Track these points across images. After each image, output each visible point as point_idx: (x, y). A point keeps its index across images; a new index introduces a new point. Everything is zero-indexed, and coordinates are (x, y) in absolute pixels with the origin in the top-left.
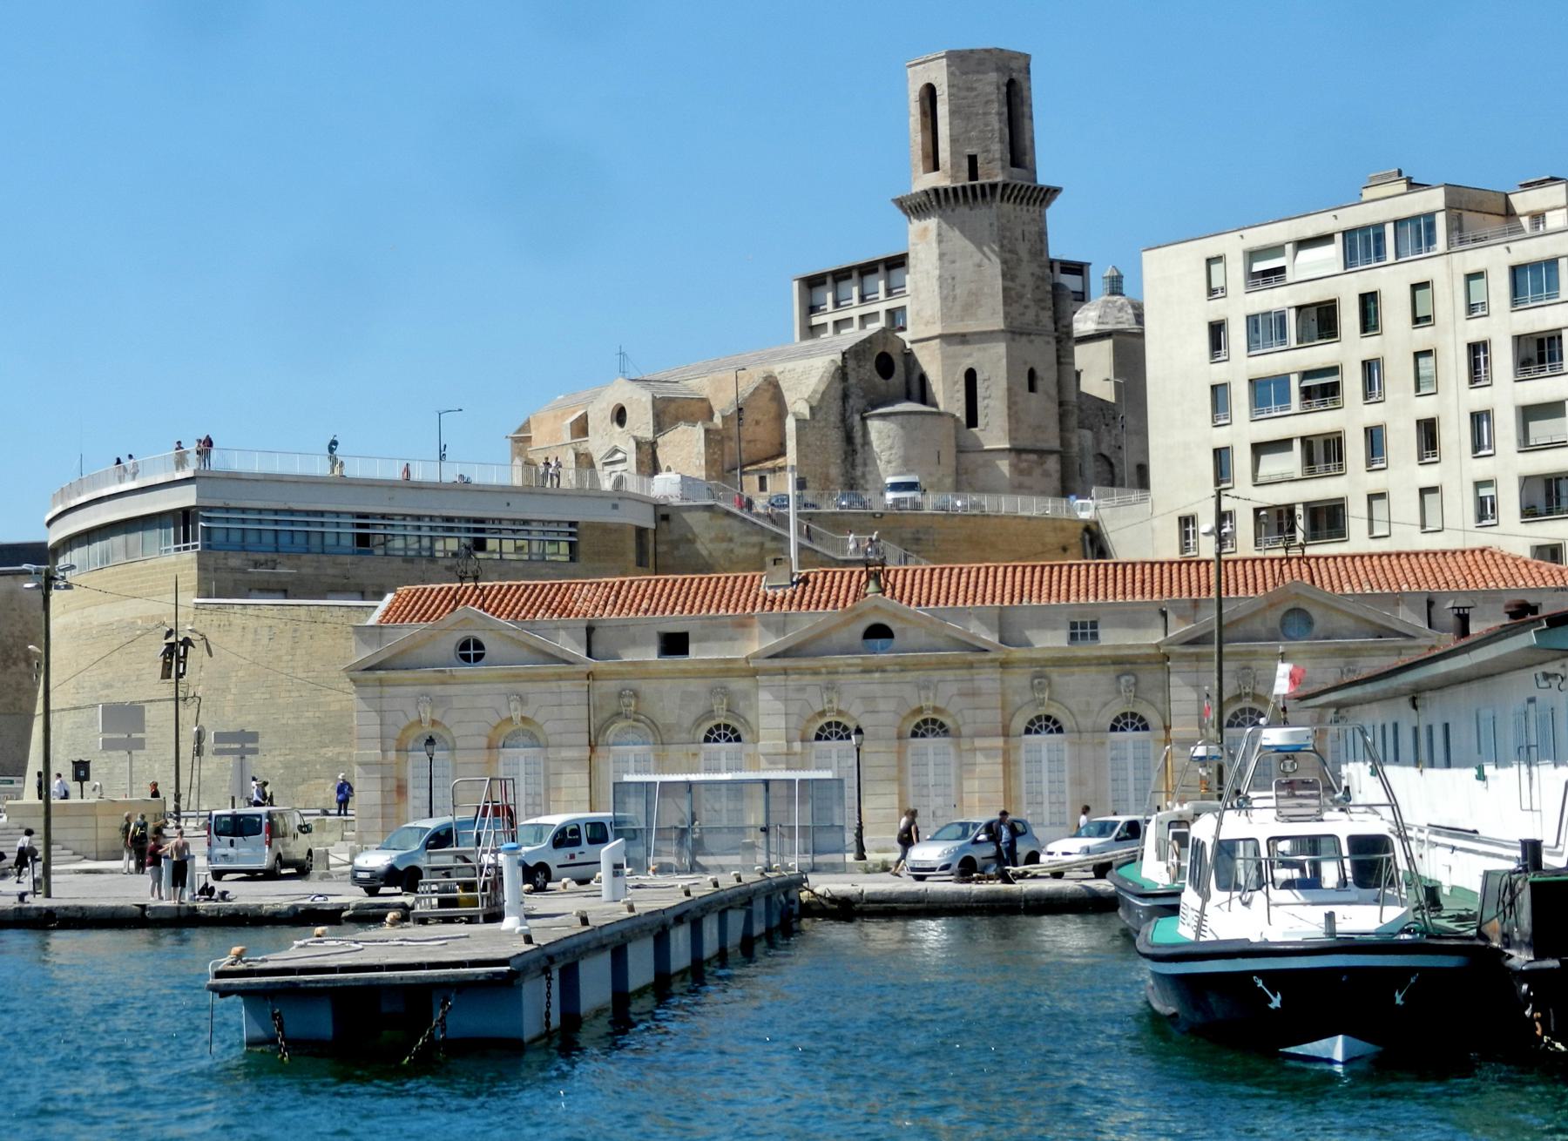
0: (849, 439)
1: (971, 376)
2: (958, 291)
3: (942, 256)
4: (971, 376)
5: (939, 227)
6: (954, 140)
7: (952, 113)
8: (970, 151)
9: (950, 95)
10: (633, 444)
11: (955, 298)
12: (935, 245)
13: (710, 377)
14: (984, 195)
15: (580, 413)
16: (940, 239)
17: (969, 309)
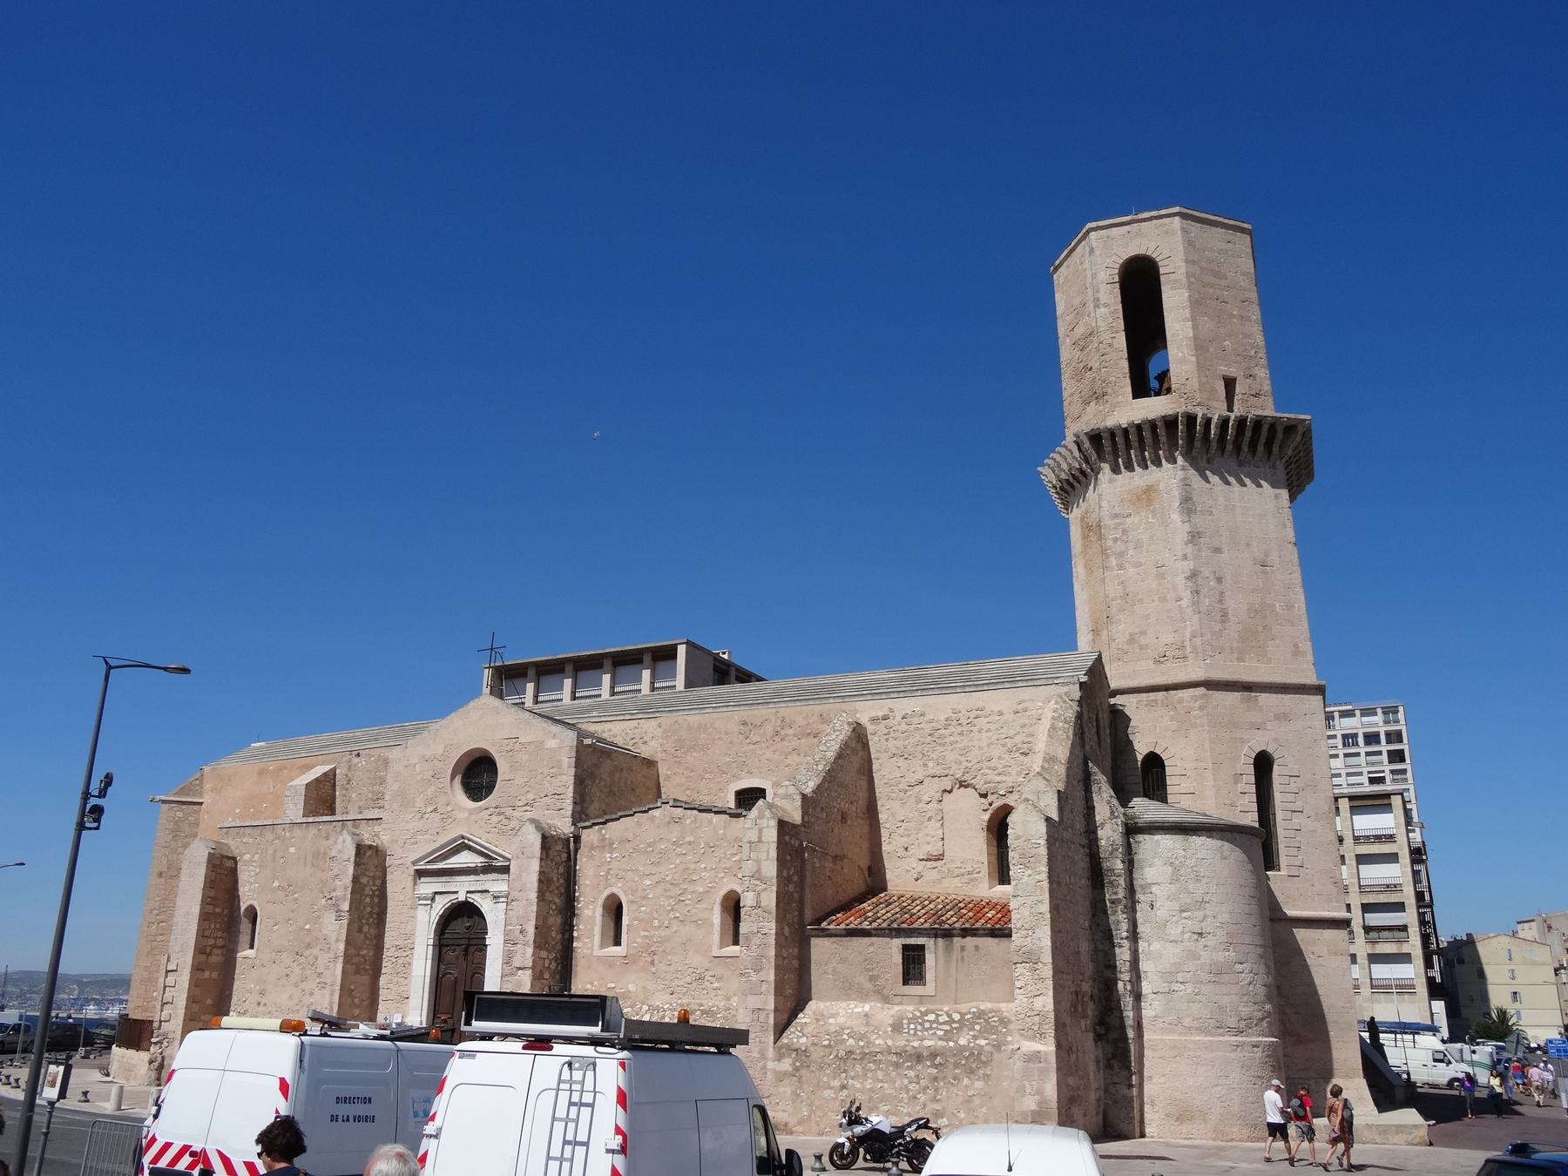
0: (1097, 875)
1: (1263, 764)
2: (1230, 604)
3: (1194, 537)
4: (1263, 764)
5: (1186, 484)
6: (1200, 345)
7: (1196, 304)
8: (1232, 371)
9: (1189, 275)
10: (535, 840)
11: (1225, 615)
12: (1176, 517)
13: (666, 719)
14: (1269, 445)
15: (327, 768)
16: (1188, 504)
17: (1253, 639)
